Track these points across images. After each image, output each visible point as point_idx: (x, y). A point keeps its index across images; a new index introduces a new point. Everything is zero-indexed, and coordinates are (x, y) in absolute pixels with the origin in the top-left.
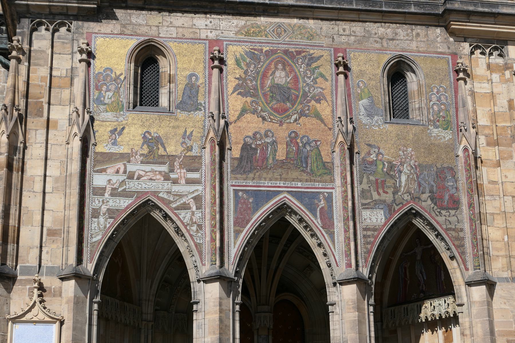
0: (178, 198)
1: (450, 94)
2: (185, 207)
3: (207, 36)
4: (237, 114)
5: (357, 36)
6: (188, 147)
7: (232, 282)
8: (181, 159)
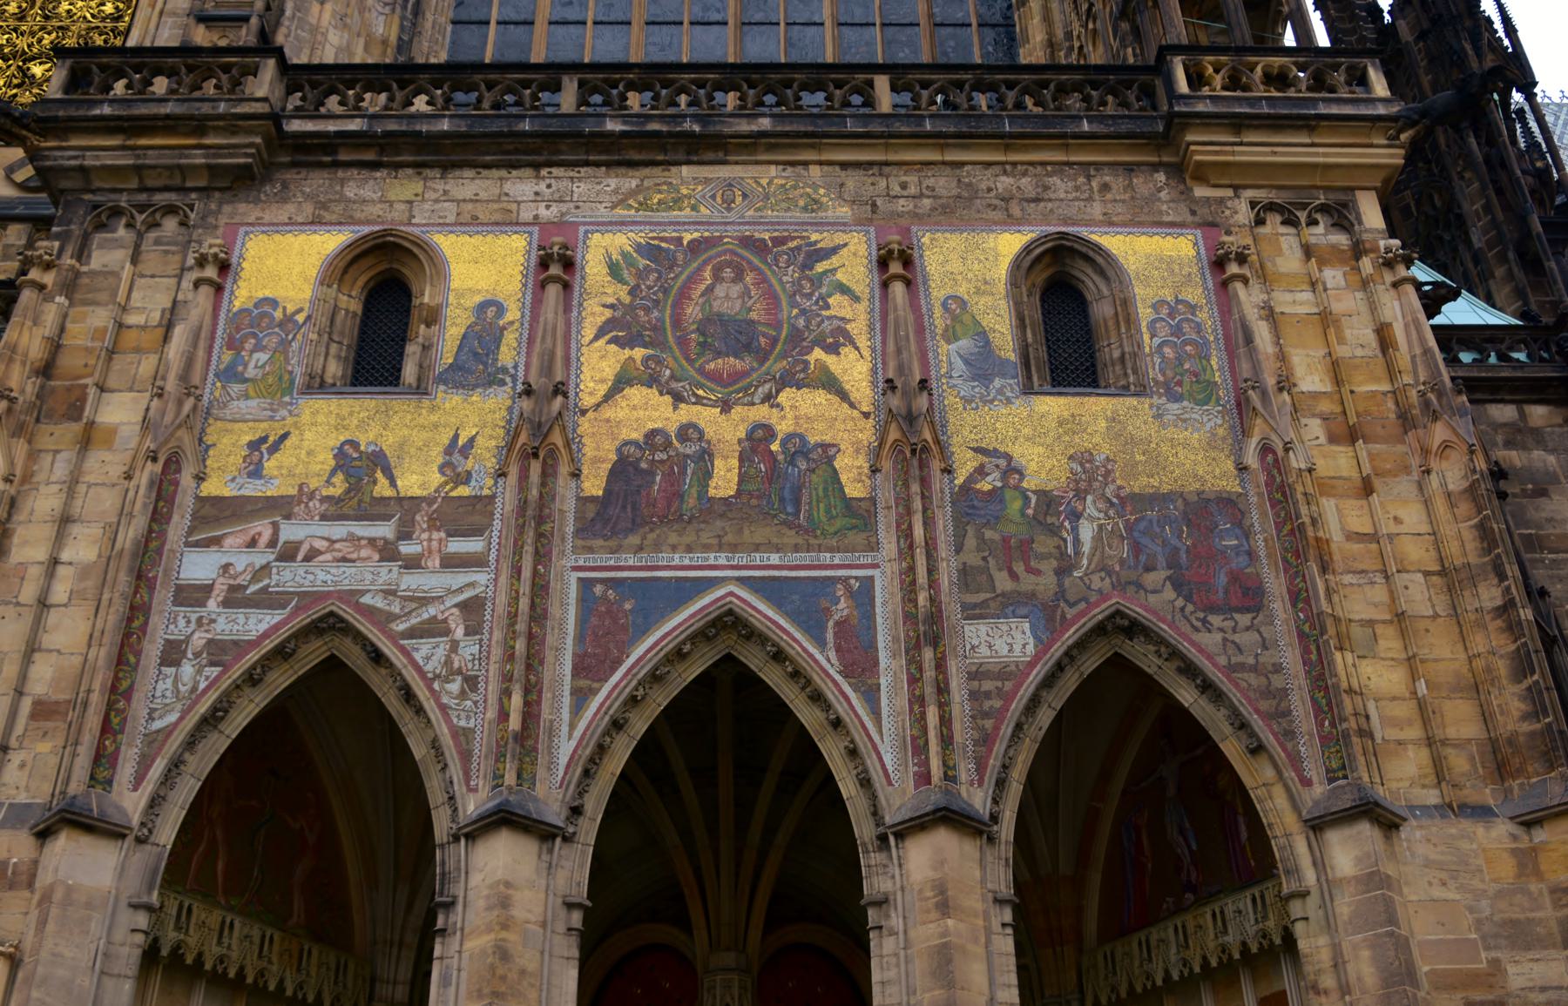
0: (414, 605)
1: (1207, 317)
2: (434, 629)
3: (536, 217)
4: (603, 389)
7: (554, 837)
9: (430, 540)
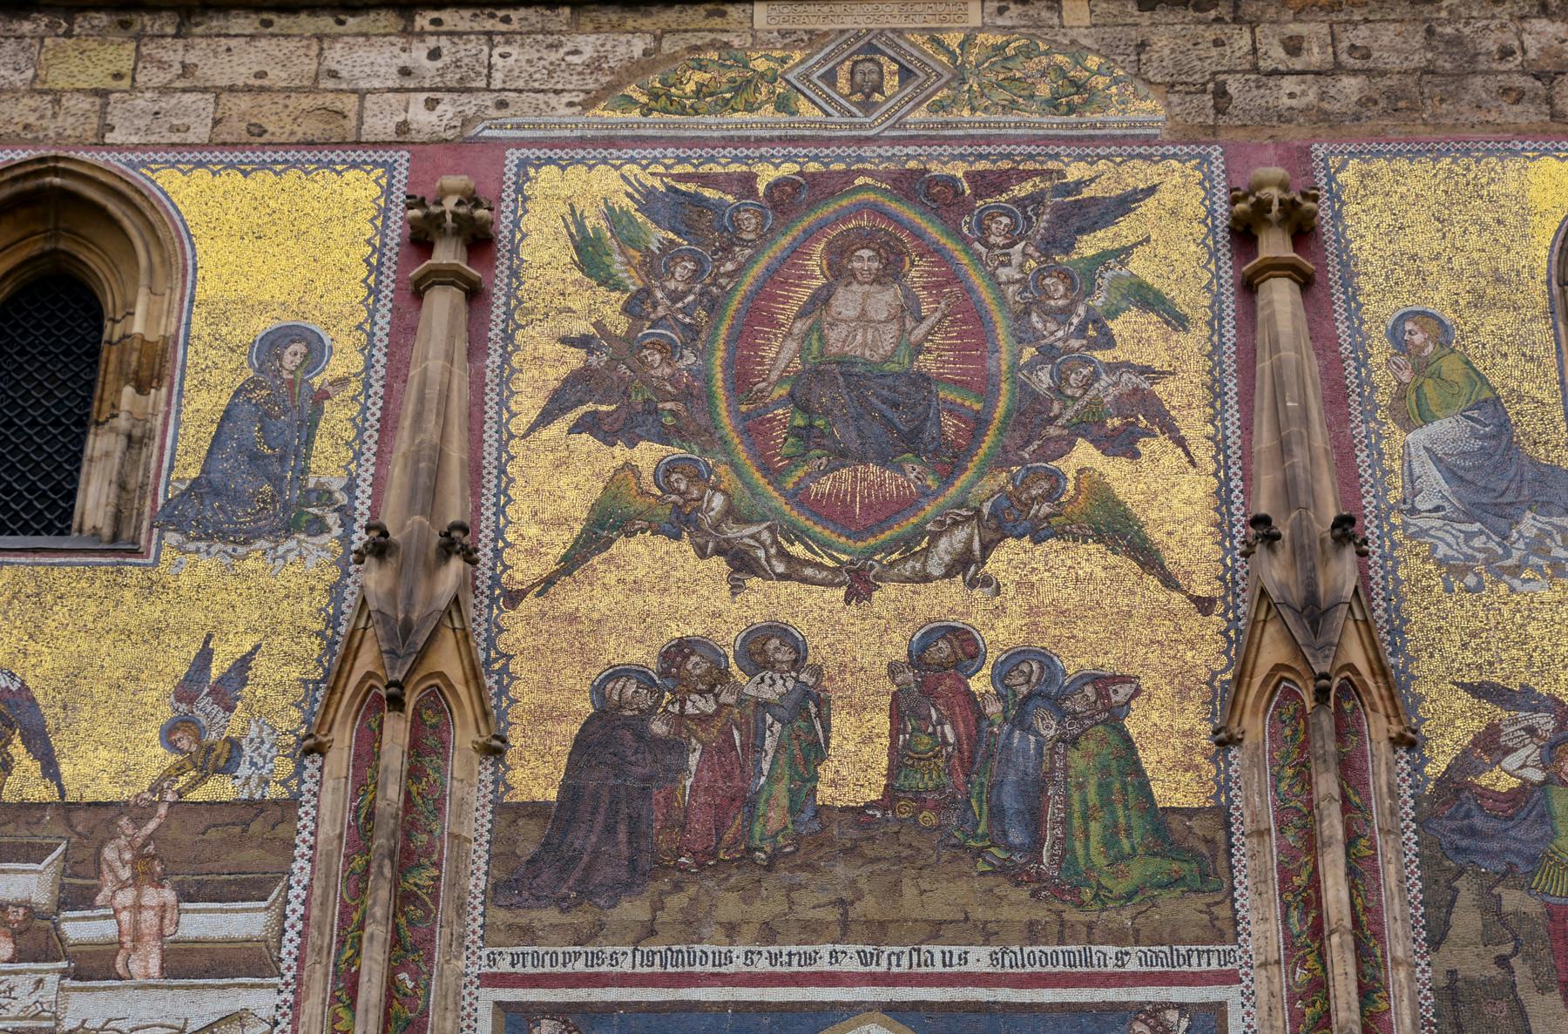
3: (403, 128)
4: (559, 542)
5: (1383, 74)
6: (210, 749)
8: (152, 826)
9: (138, 908)
